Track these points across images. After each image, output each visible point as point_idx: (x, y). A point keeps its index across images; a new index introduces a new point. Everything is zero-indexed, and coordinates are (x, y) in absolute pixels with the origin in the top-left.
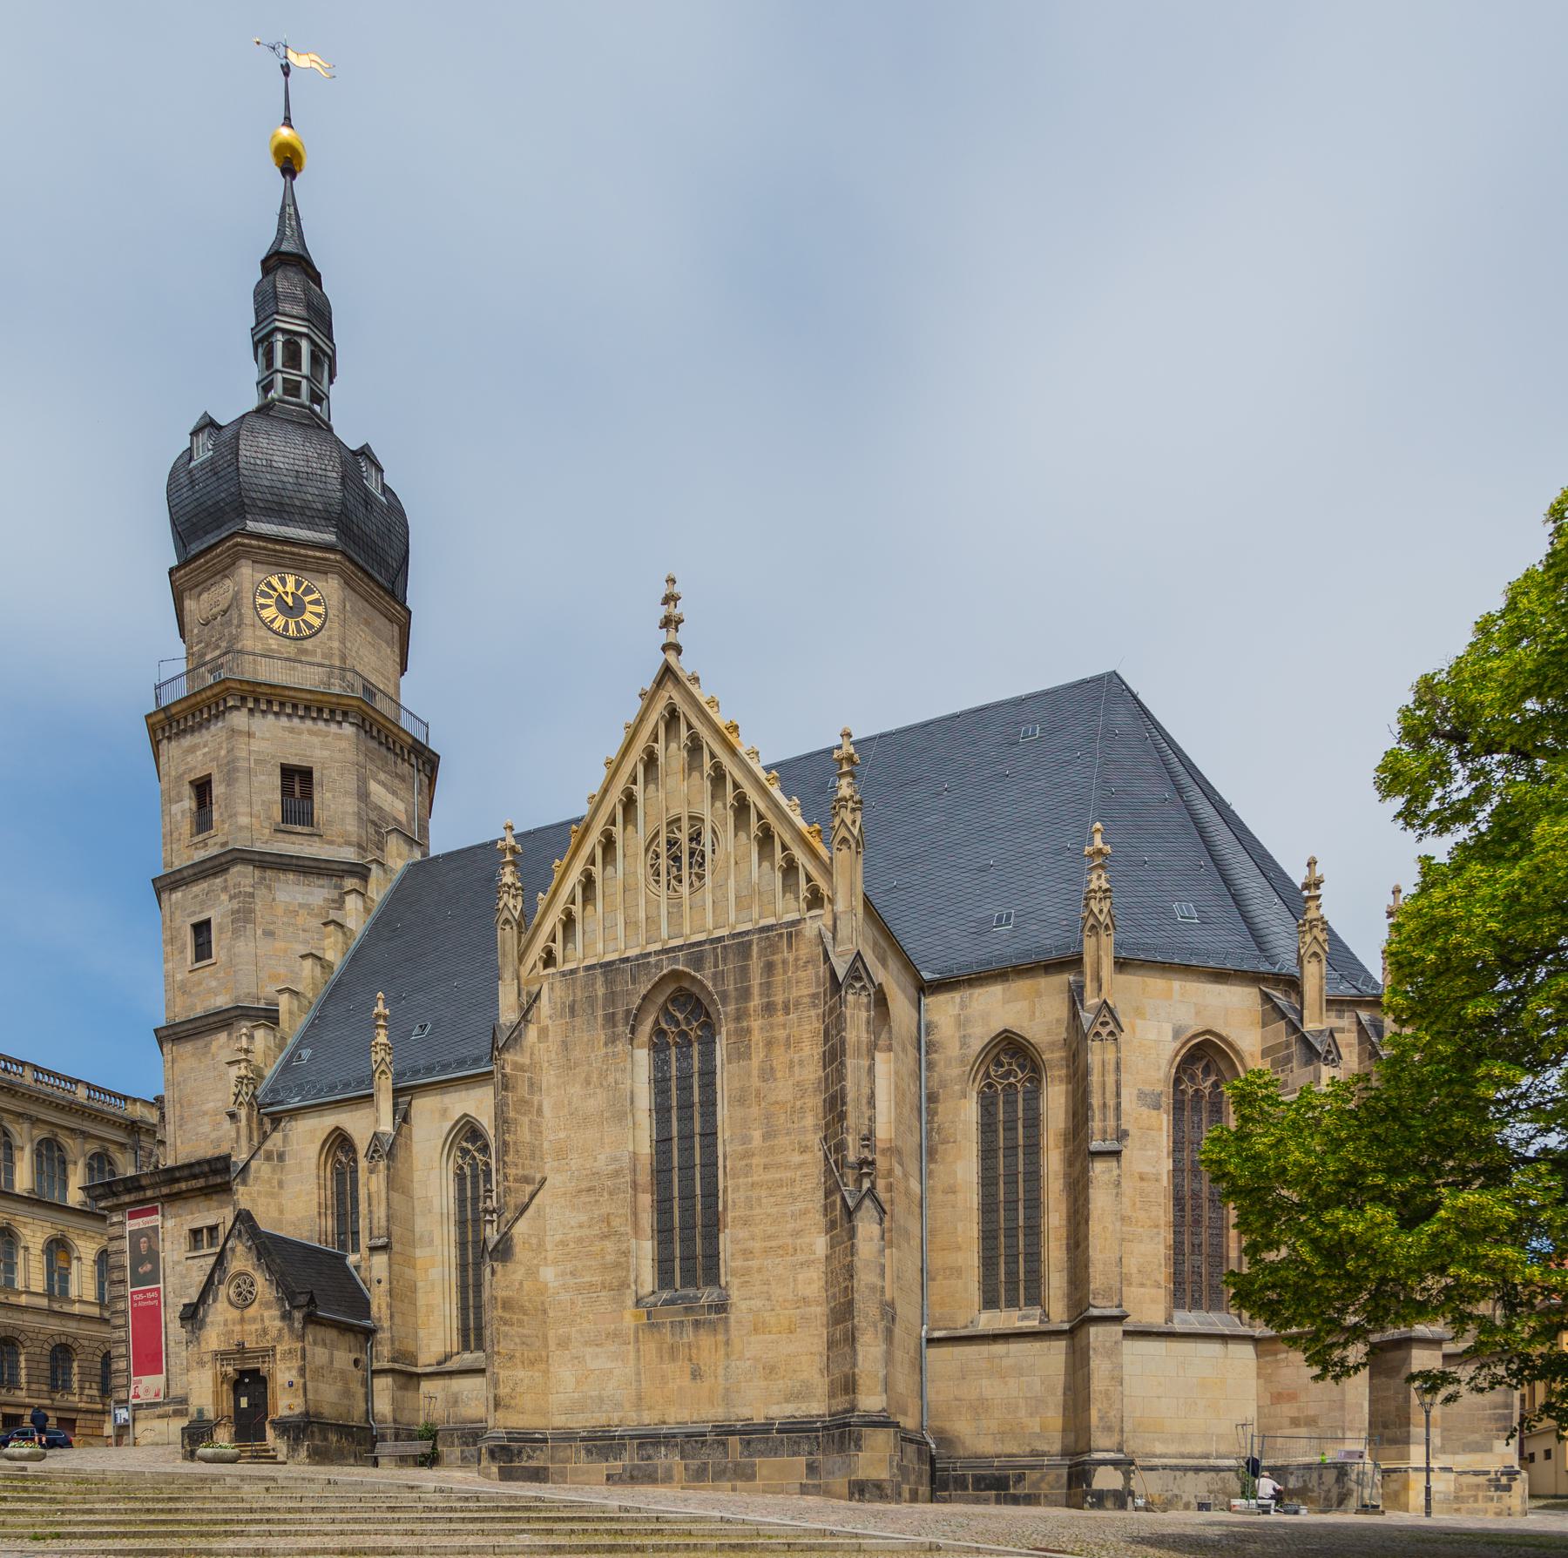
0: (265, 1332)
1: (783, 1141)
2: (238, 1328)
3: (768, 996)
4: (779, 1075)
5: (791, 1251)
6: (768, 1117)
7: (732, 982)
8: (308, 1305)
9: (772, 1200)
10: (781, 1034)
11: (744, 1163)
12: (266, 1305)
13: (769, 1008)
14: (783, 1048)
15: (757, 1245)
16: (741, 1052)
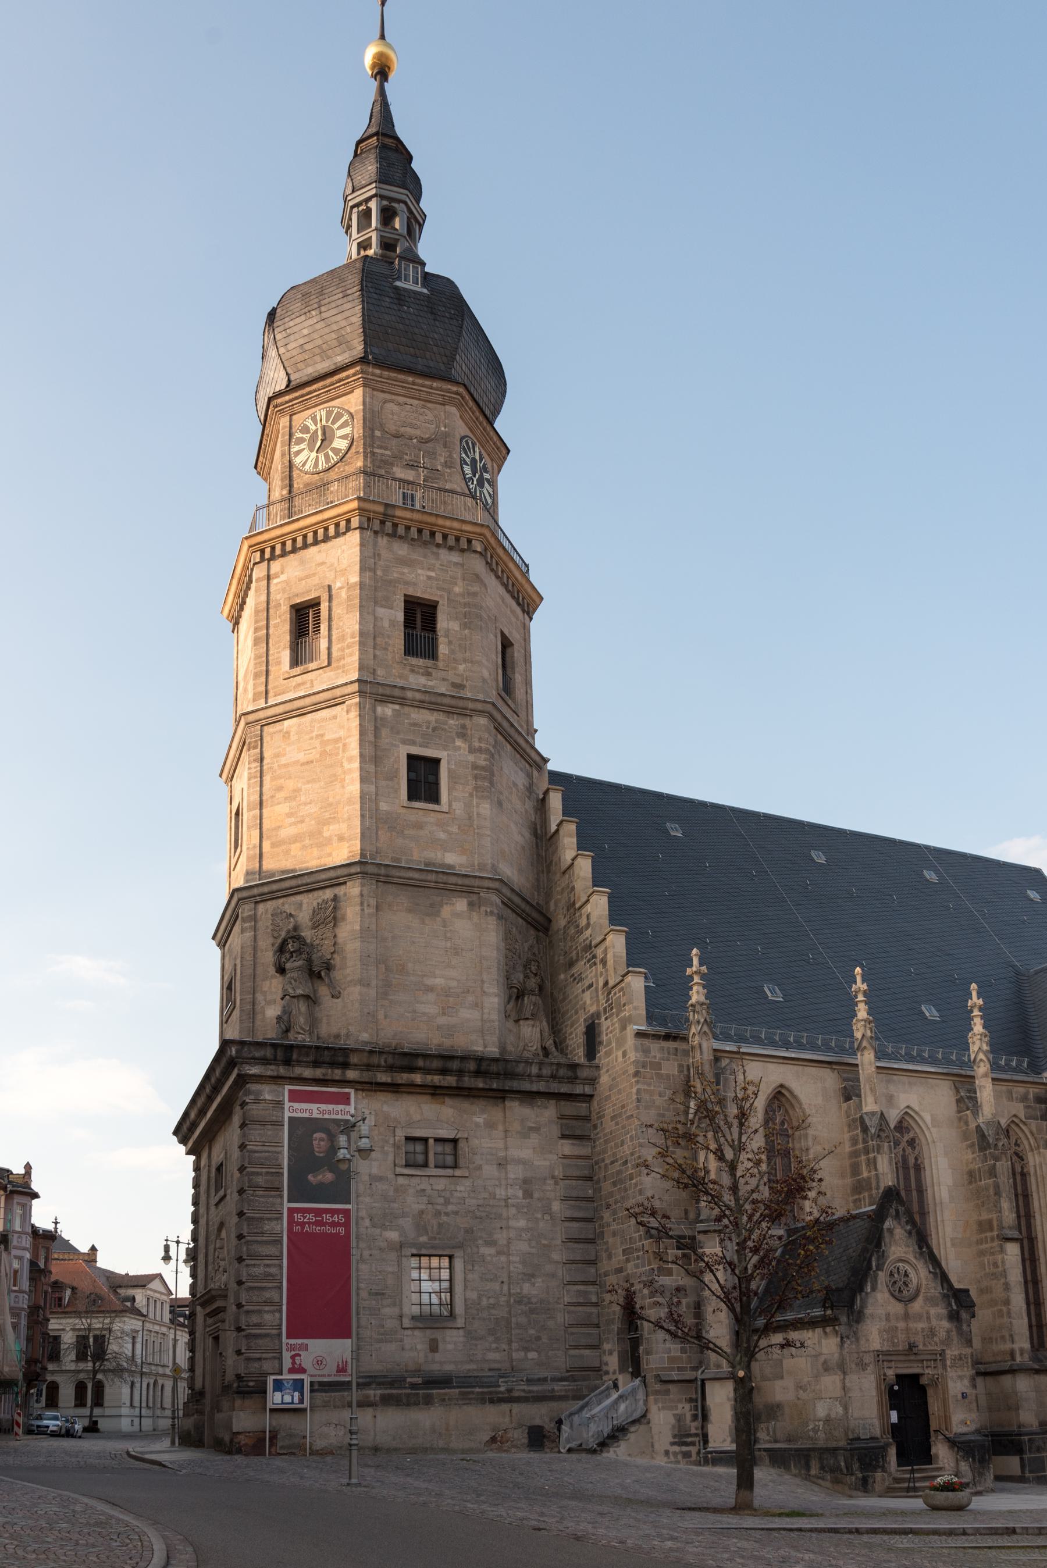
0: (932, 1332)
2: (901, 1325)
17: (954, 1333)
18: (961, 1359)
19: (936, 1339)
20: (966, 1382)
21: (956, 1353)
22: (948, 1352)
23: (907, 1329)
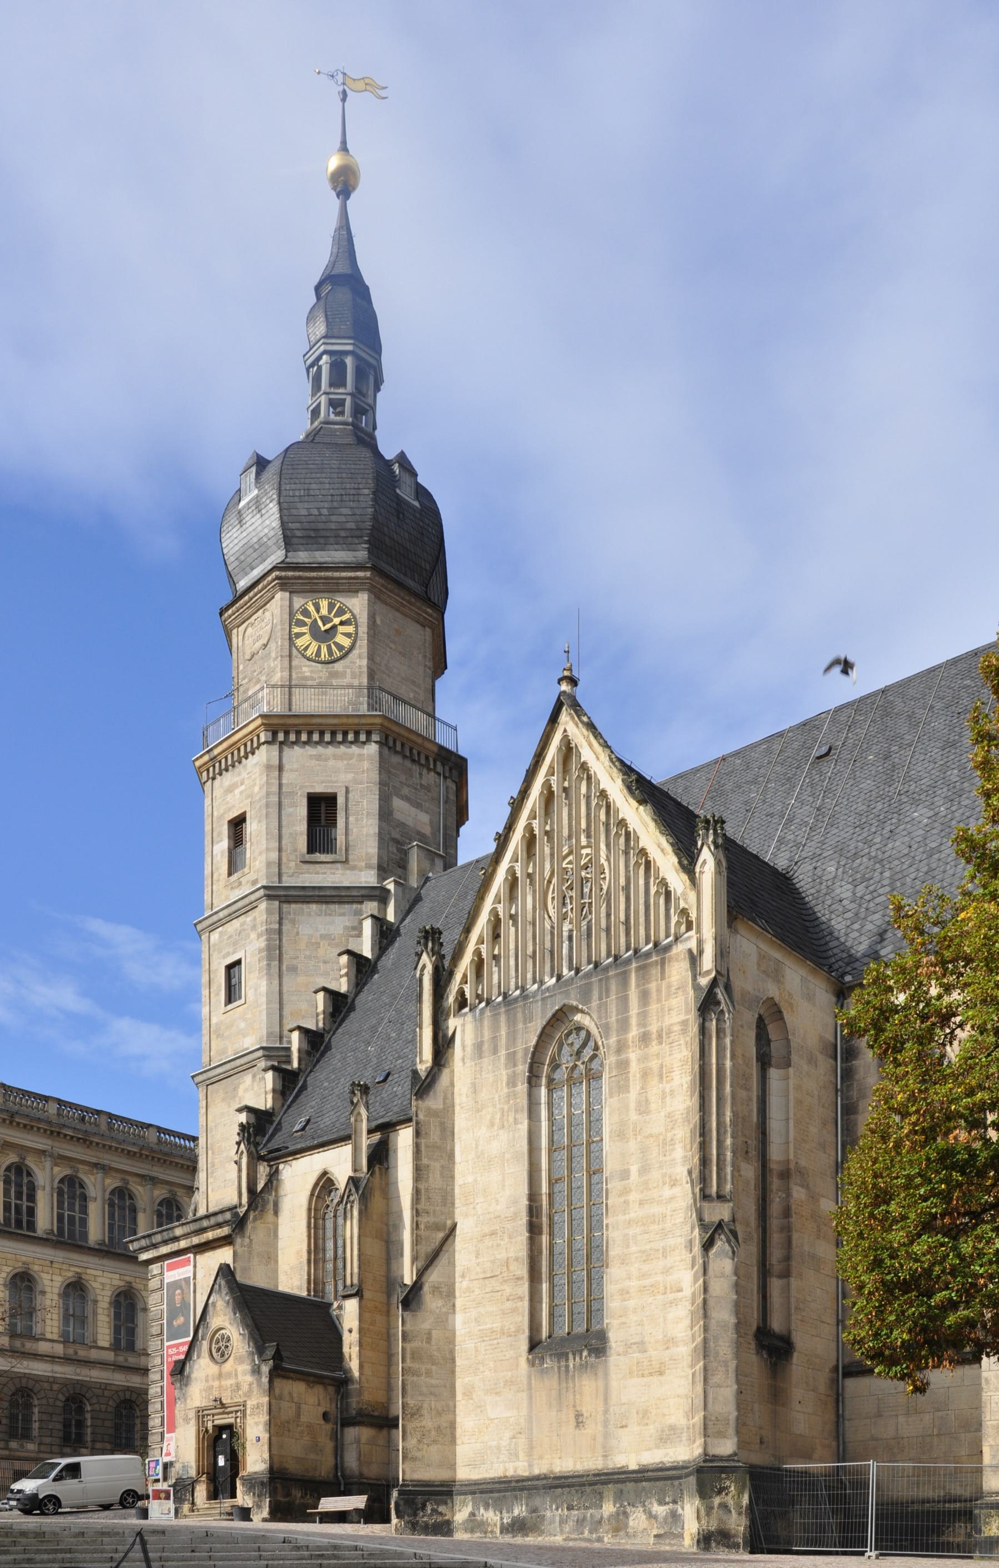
0: (238, 1387)
1: (655, 1175)
2: (216, 1384)
3: (644, 1026)
4: (653, 1106)
5: (662, 1289)
6: (644, 1150)
7: (614, 1014)
8: (273, 1358)
9: (646, 1236)
10: (654, 1064)
11: (622, 1199)
12: (240, 1360)
13: (645, 1038)
14: (656, 1079)
15: (634, 1284)
16: (622, 1087)
17: (255, 1386)
18: (258, 1407)
19: (240, 1392)
20: (261, 1427)
21: (255, 1402)
22: (249, 1404)
23: (220, 1387)
